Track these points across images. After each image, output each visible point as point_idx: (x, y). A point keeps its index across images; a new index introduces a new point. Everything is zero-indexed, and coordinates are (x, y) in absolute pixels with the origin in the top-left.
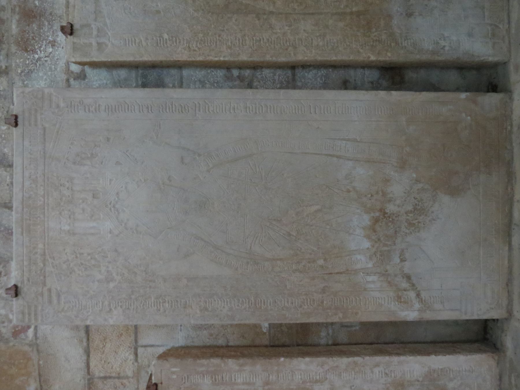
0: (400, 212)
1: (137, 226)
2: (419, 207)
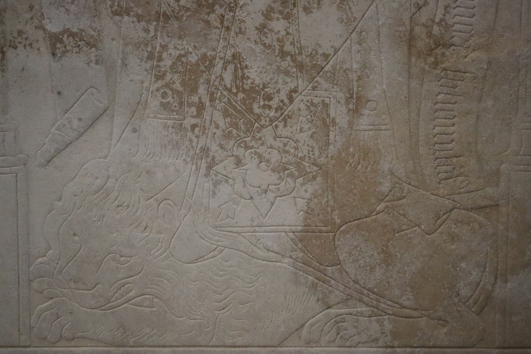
0: (241, 32)
2: (257, 110)
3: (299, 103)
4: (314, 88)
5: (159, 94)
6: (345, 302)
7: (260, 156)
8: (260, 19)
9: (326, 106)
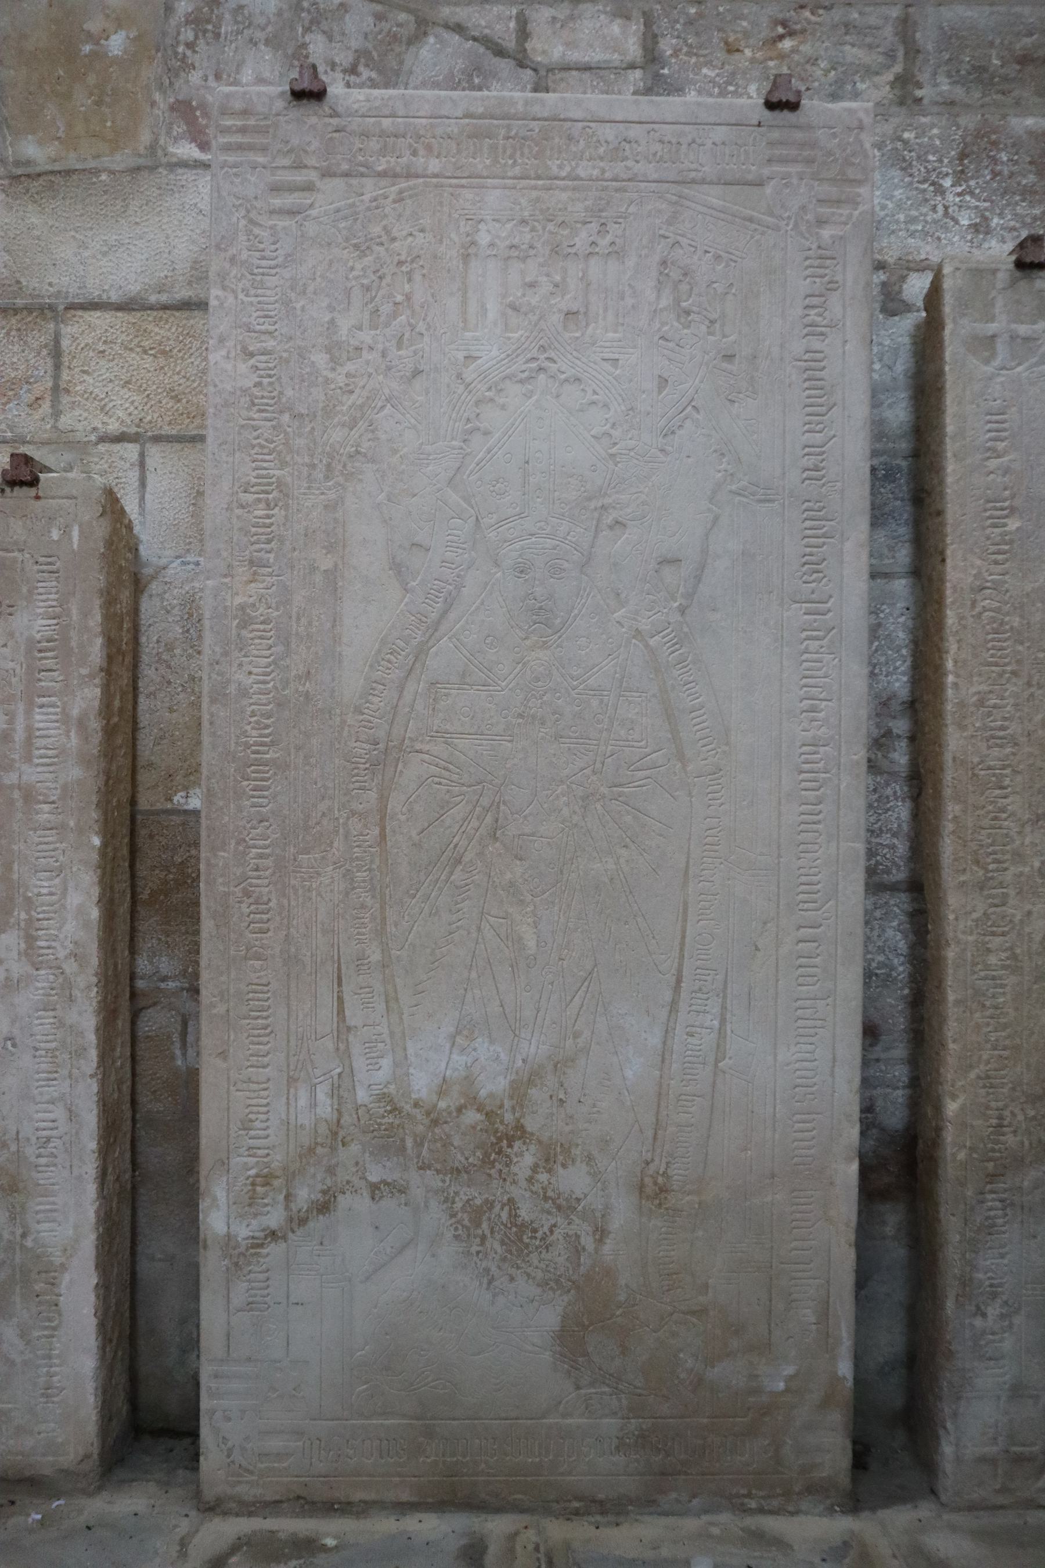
0: (514, 1182)
1: (486, 433)
3: (558, 1233)
4: (569, 1224)
5: (452, 1229)
6: (592, 1384)
7: (528, 1275)
8: (529, 1173)
9: (578, 1237)
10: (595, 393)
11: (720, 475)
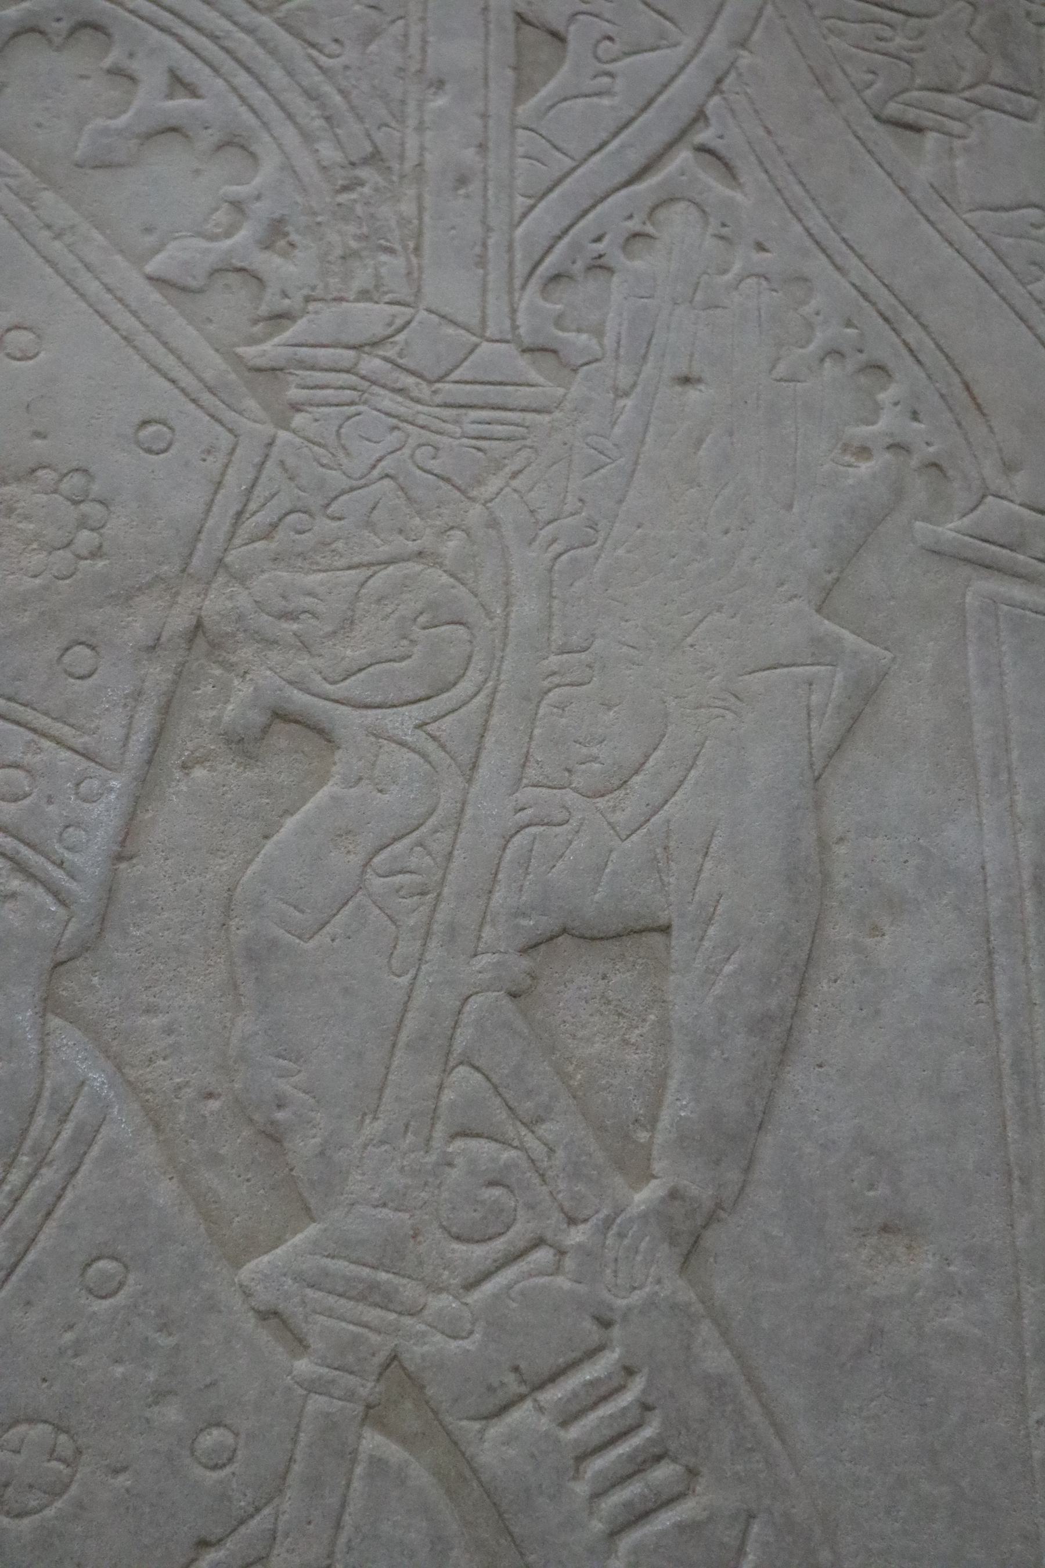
10: (179, 83)
11: (865, 468)
